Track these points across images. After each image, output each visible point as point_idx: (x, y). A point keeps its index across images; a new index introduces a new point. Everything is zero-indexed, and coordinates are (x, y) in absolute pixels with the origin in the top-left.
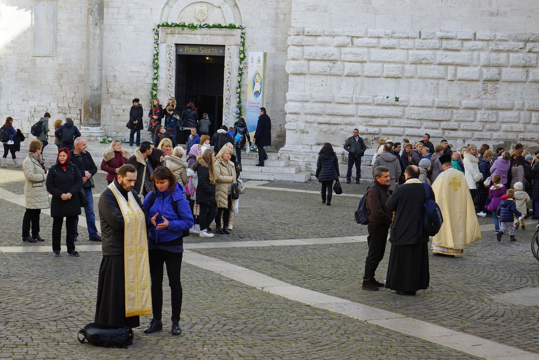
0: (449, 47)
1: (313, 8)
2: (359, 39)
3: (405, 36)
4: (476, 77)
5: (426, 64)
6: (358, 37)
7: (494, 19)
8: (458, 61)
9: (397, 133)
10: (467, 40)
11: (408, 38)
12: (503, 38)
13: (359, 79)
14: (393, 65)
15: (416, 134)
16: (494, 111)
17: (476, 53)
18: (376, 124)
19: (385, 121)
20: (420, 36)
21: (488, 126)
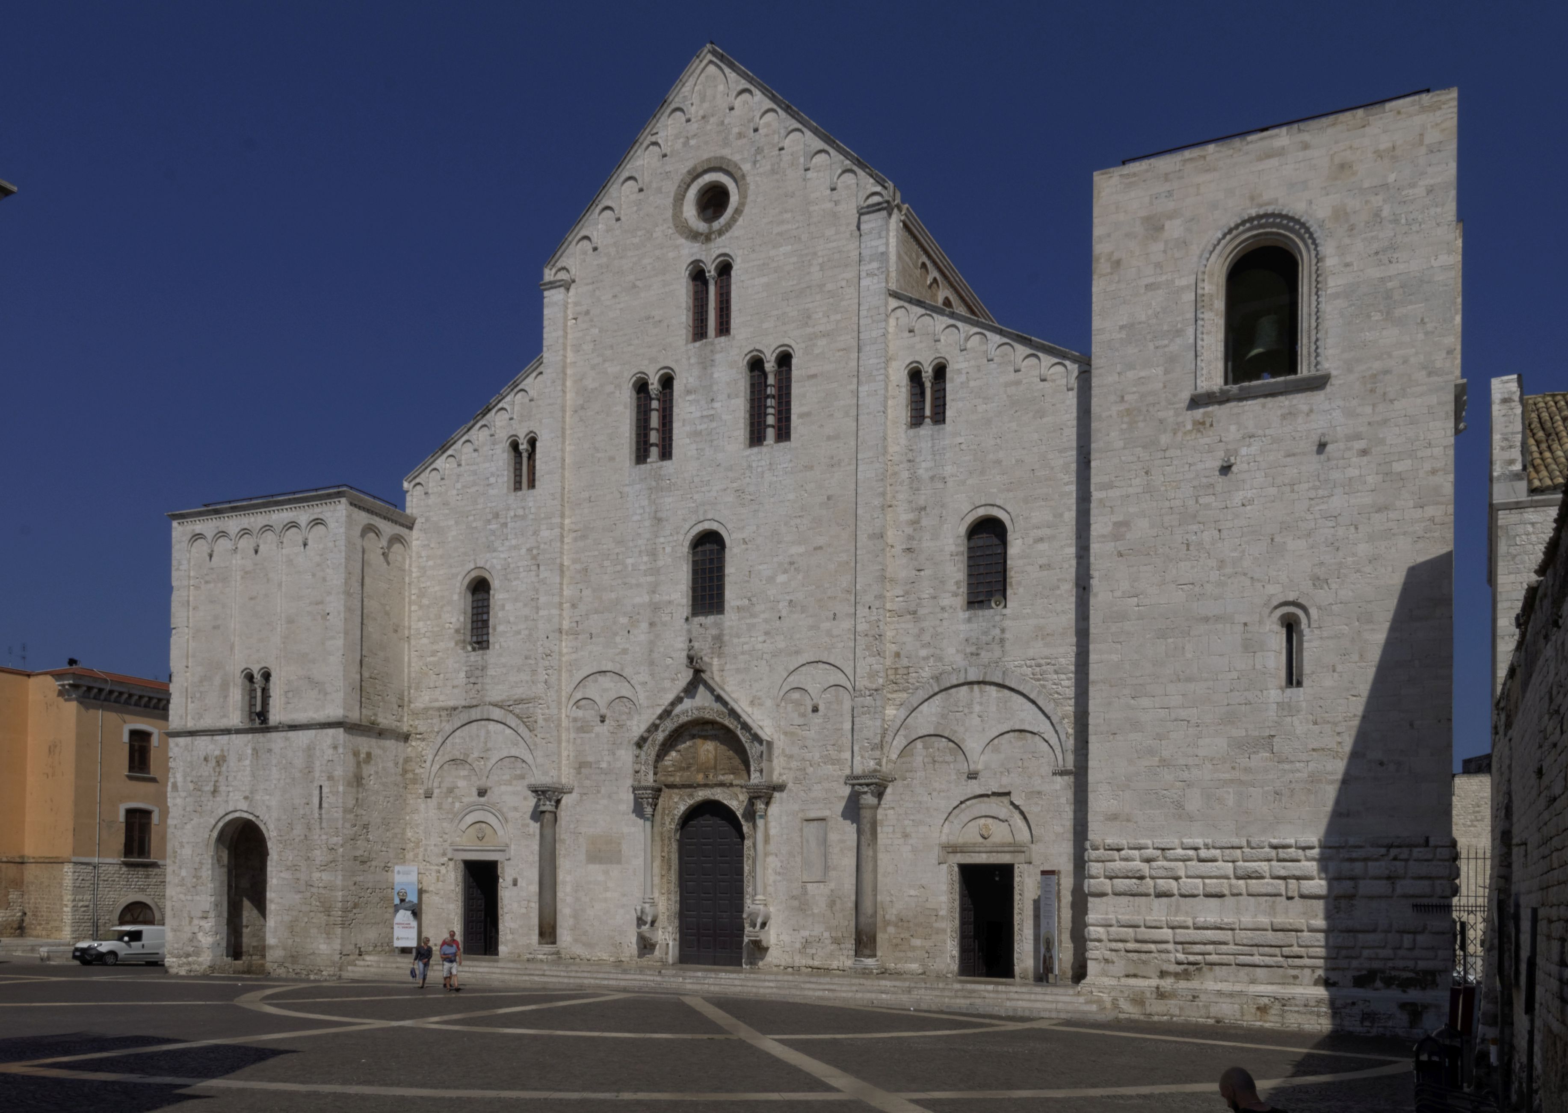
8: (1297, 873)
13: (1173, 899)
14: (1215, 881)
18: (1198, 951)
19: (1210, 948)
21: (1344, 953)
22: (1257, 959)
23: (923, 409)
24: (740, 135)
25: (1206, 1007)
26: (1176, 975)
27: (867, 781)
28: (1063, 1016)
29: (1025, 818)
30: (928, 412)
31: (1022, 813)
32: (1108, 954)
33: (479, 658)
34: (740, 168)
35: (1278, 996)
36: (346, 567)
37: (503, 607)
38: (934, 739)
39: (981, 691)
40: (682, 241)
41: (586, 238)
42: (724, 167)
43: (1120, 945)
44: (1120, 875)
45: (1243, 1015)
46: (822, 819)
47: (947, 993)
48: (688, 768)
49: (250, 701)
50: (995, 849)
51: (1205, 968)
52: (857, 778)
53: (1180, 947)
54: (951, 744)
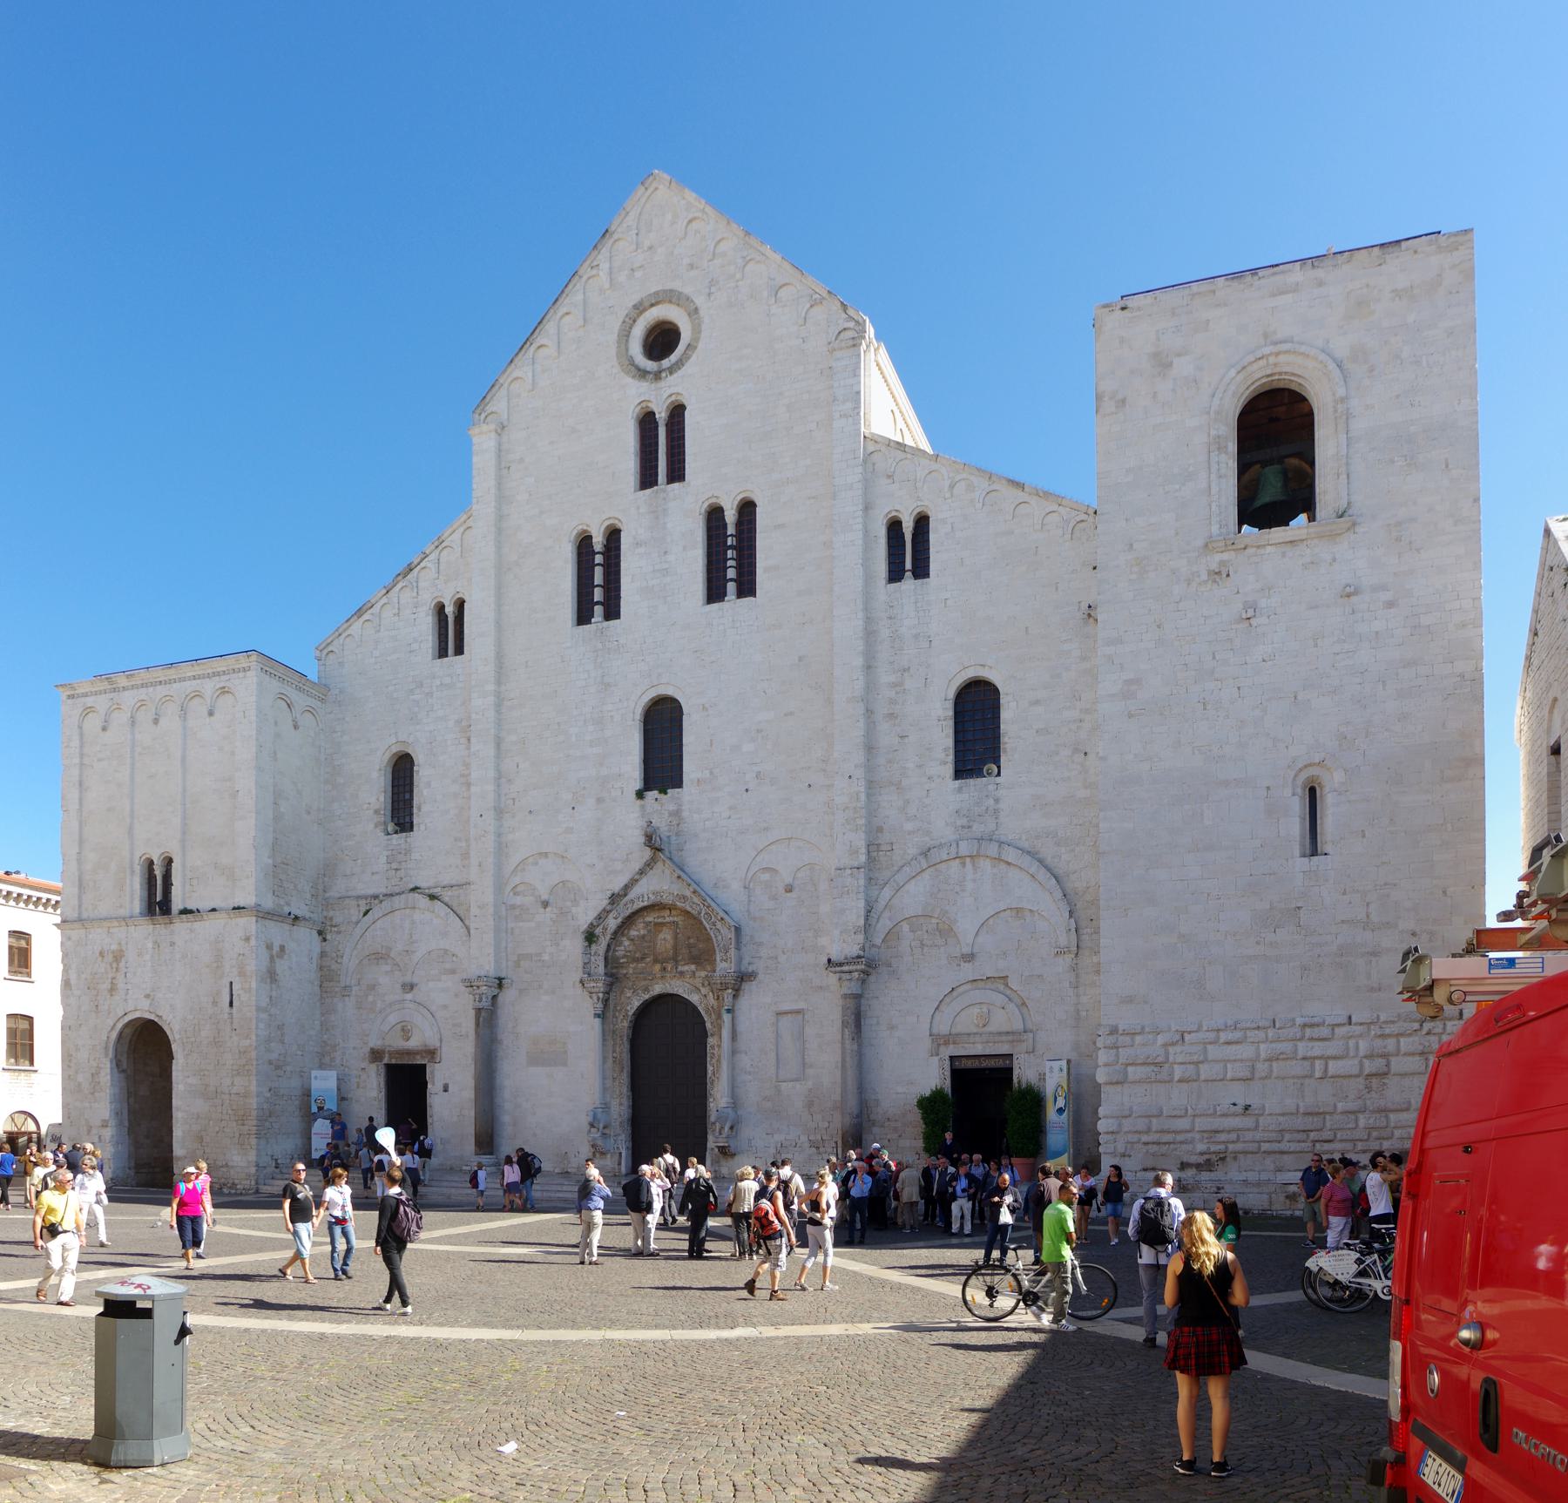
0: (1316, 1036)
1: (1129, 1000)
2: (1193, 1034)
4: (1355, 1071)
5: (1284, 1059)
6: (1190, 1033)
9: (1251, 1149)
10: (1338, 1025)
11: (1258, 1028)
15: (1277, 1149)
16: (1384, 1114)
17: (1352, 1043)
21: (1375, 1134)
22: (1284, 1146)
33: (403, 841)
36: (257, 740)
37: (428, 784)
40: (629, 380)
46: (798, 1012)
48: (643, 958)
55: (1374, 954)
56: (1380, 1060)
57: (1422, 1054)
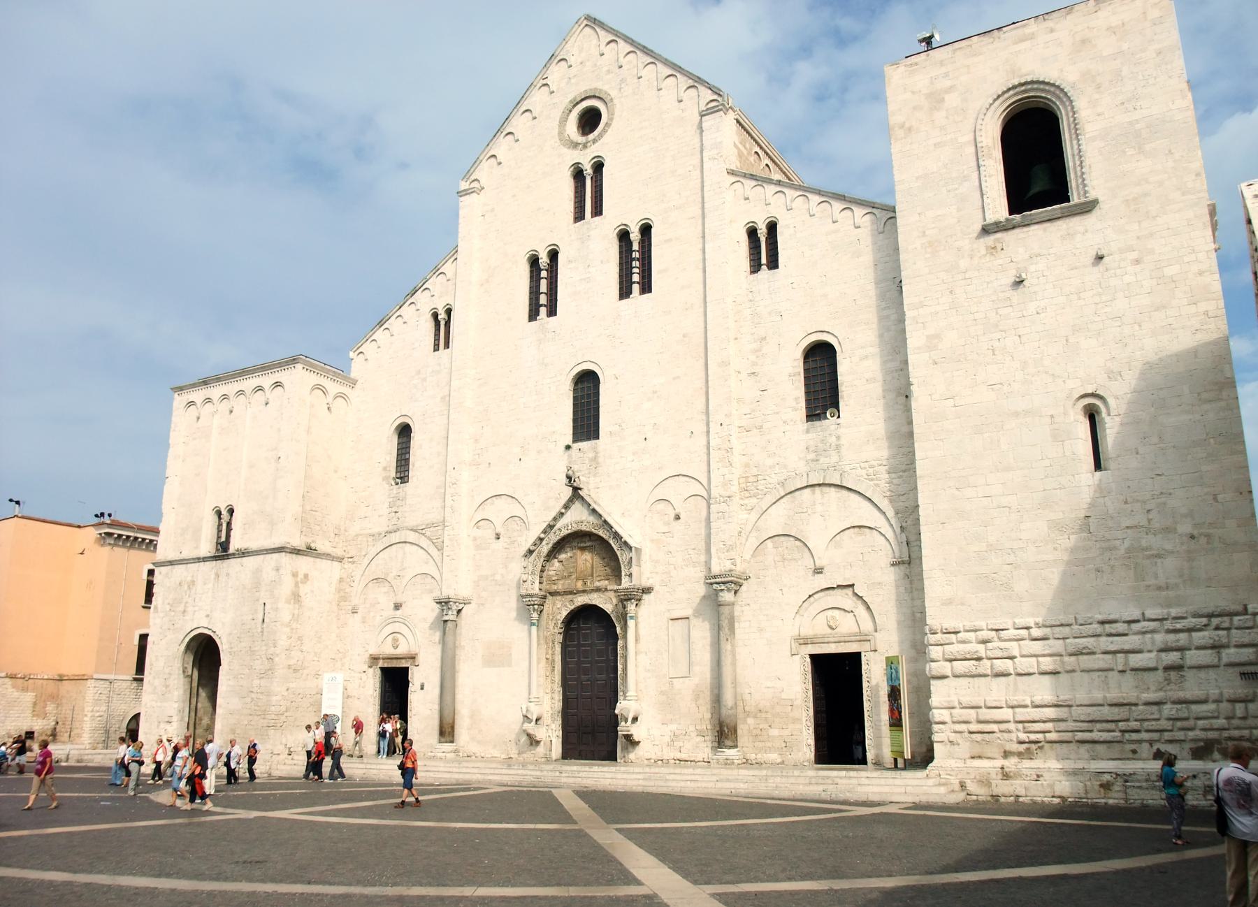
0: (1113, 631)
1: (949, 602)
3: (1058, 623)
4: (1152, 665)
7: (1164, 593)
12: (1180, 615)
15: (1088, 739)
16: (1184, 705)
17: (1149, 636)
18: (1038, 729)
20: (1076, 622)
22: (1096, 735)
23: (760, 258)
24: (609, 72)
25: (1051, 786)
26: (1020, 754)
27: (723, 580)
28: (910, 799)
29: (868, 608)
30: (764, 261)
31: (865, 603)
32: (953, 737)
34: (609, 95)
35: (1120, 772)
38: (782, 538)
39: (823, 493)
41: (494, 156)
42: (597, 95)
43: (963, 727)
44: (959, 657)
45: (1086, 792)
47: (801, 780)
49: (218, 534)
50: (842, 639)
51: (1047, 746)
52: (715, 577)
53: (1020, 726)
54: (798, 543)
55: (1158, 556)
56: (1175, 653)
57: (1213, 647)
